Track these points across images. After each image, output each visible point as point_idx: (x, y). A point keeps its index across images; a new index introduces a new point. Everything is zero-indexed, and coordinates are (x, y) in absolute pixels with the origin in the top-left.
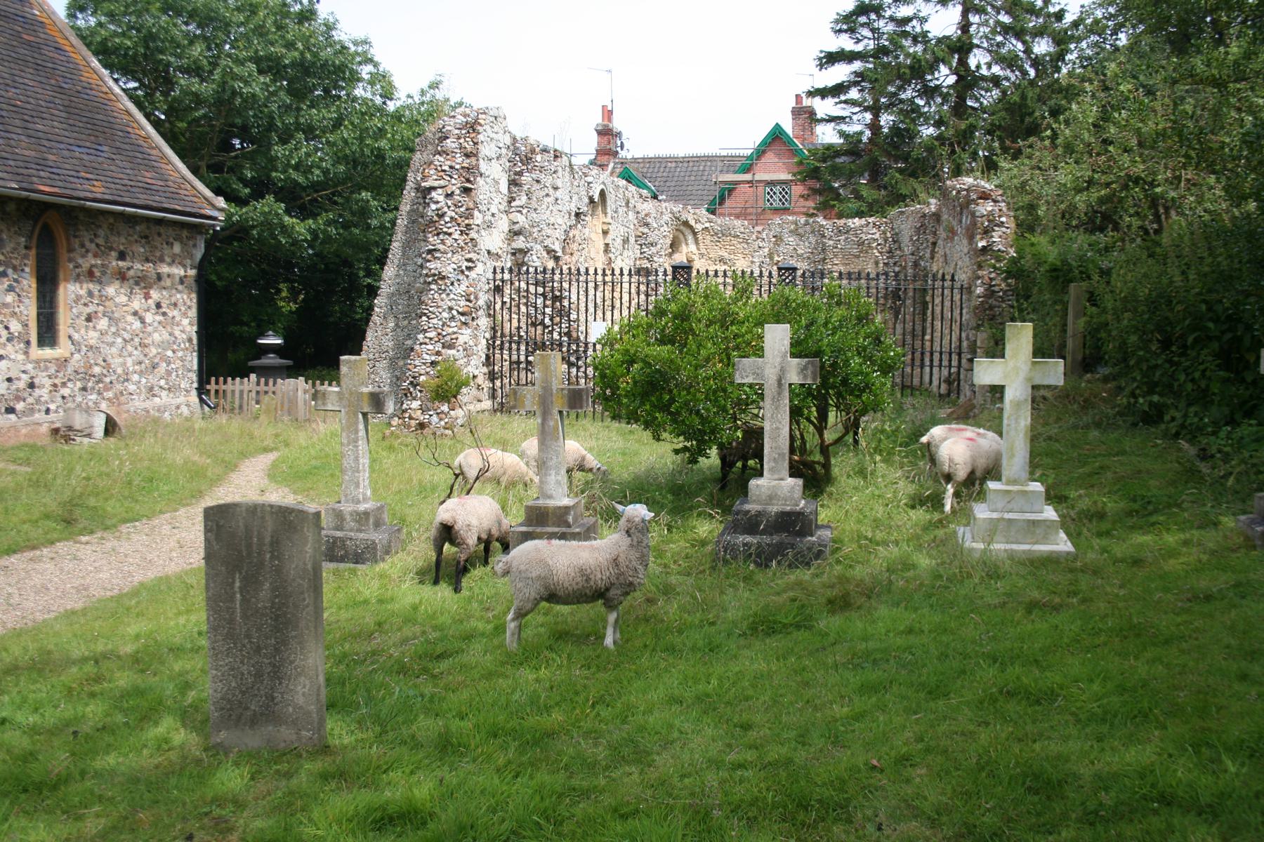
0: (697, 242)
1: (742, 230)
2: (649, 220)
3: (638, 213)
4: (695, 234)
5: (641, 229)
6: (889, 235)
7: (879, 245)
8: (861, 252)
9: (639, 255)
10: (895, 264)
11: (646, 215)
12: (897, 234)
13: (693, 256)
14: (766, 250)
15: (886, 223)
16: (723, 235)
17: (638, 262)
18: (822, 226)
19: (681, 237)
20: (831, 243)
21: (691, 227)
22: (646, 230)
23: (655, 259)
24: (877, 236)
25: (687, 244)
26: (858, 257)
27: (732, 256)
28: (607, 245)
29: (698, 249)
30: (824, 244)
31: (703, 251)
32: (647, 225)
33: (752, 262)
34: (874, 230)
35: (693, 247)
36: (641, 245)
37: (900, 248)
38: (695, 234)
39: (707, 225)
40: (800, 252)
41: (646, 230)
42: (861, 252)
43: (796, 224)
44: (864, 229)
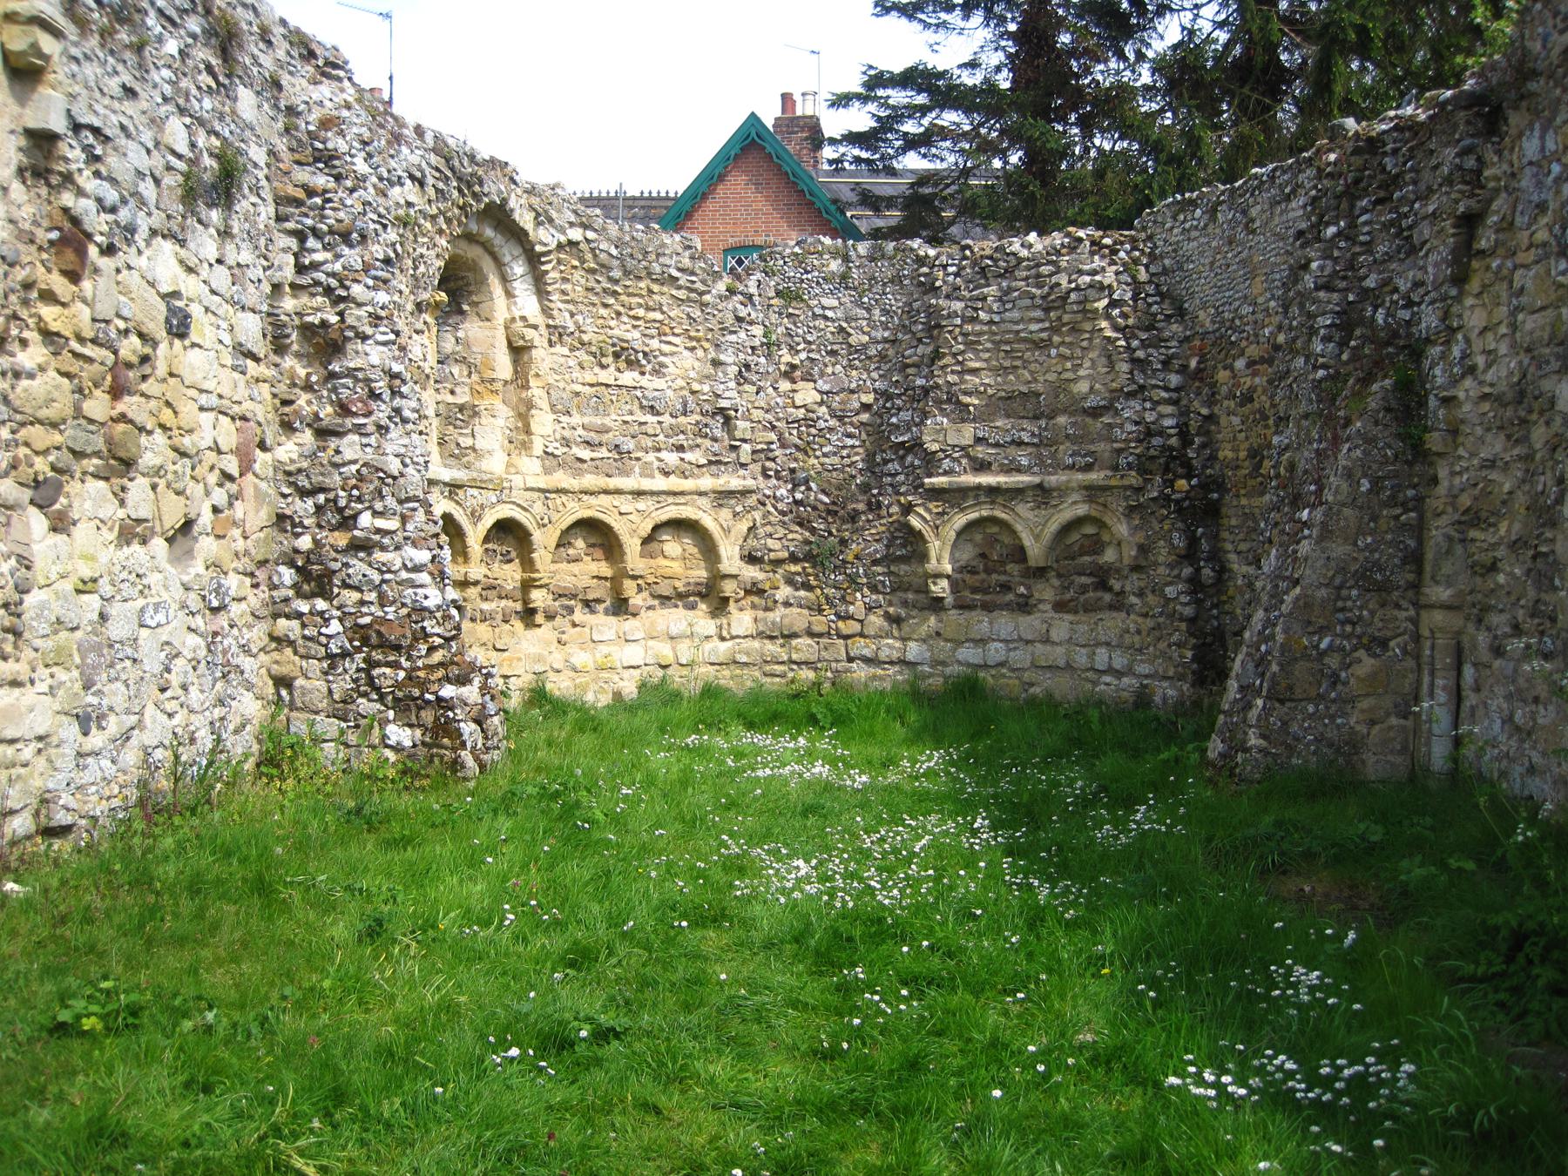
0: (541, 291)
1: (686, 262)
2: (338, 143)
3: (291, 111)
4: (534, 260)
5: (303, 175)
6: (1143, 275)
7: (1113, 304)
8: (1054, 330)
9: (289, 273)
10: (1166, 363)
11: (326, 124)
12: (1165, 272)
13: (530, 334)
14: (758, 331)
15: (1133, 240)
16: (627, 273)
17: (289, 304)
18: (921, 261)
19: (487, 265)
20: (958, 306)
21: (518, 235)
22: (321, 181)
23: (357, 290)
24: (1109, 278)
25: (509, 294)
26: (1041, 345)
27: (655, 344)
28: (41, 141)
29: (547, 312)
30: (933, 312)
31: (564, 319)
32: (326, 159)
33: (716, 363)
34: (1097, 262)
35: (527, 303)
36: (300, 236)
37: (1181, 313)
38: (534, 260)
39: (576, 234)
40: (857, 338)
41: (321, 181)
42: (1054, 330)
43: (846, 259)
44: (1064, 261)
